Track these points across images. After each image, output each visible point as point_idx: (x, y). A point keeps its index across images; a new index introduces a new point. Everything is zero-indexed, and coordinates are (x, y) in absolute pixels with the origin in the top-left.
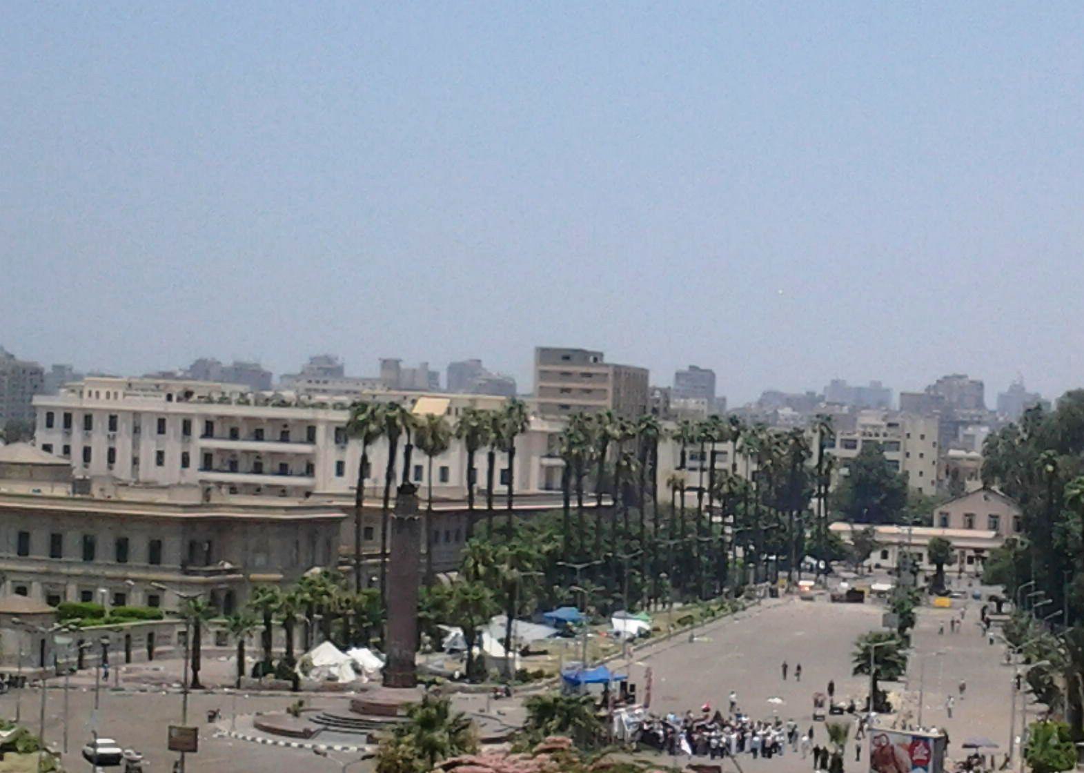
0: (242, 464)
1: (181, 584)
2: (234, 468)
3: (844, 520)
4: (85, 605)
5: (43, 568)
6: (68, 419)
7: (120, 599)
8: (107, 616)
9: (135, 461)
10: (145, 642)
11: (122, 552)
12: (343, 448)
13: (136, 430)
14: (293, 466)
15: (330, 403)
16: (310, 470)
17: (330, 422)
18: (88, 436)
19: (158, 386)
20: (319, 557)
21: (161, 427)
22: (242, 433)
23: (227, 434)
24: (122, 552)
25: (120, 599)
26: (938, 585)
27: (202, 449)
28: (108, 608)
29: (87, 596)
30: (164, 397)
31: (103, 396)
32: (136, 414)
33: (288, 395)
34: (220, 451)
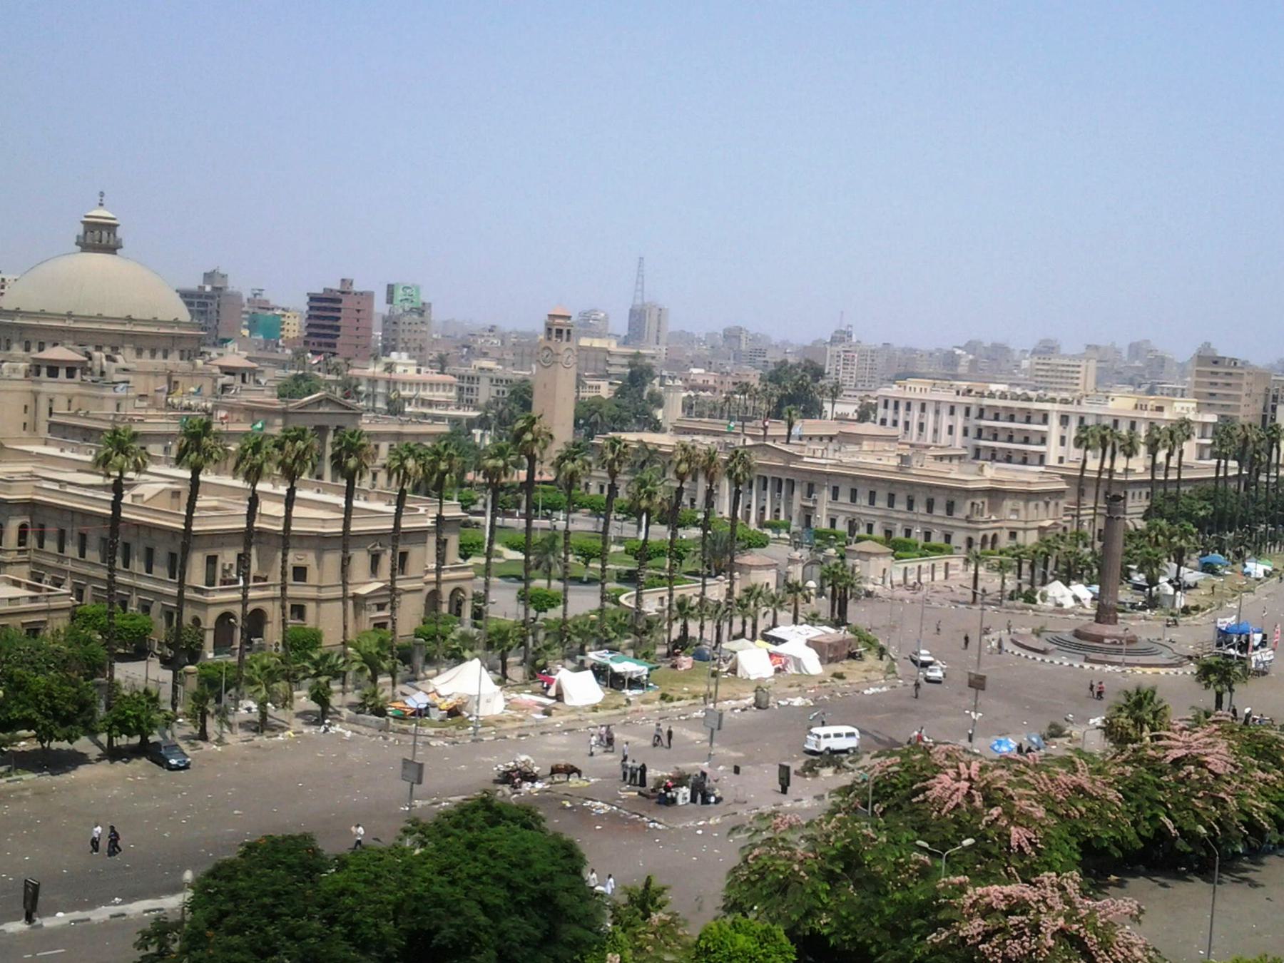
4: (907, 540)
7: (928, 536)
20: (1051, 516)
24: (930, 506)
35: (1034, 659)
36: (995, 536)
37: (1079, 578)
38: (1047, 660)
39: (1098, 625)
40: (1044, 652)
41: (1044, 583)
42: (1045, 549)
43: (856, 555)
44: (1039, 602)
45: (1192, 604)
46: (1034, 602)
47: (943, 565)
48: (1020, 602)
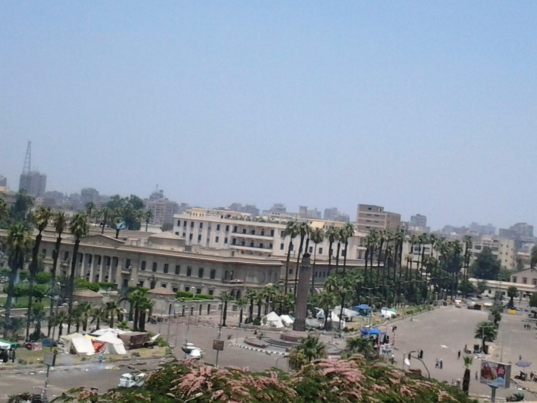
0: (247, 243)
1: (222, 287)
2: (243, 244)
3: (474, 277)
4: (186, 292)
5: (172, 278)
6: (185, 223)
7: (199, 291)
8: (194, 297)
9: (208, 240)
10: (207, 308)
11: (201, 273)
12: (284, 239)
13: (209, 228)
14: (265, 245)
15: (280, 222)
16: (271, 246)
17: (279, 229)
18: (192, 229)
19: (218, 212)
20: (272, 280)
21: (218, 228)
22: (247, 231)
23: (242, 231)
24: (201, 273)
25: (199, 291)
26: (511, 305)
27: (233, 236)
28: (194, 294)
29: (187, 289)
30: (220, 217)
31: (198, 215)
32: (210, 222)
33: (265, 218)
34: (239, 238)
35: (256, 350)
36: (239, 292)
37: (286, 313)
38: (264, 351)
39: (294, 331)
40: (263, 347)
41: (266, 314)
42: (267, 294)
43: (153, 296)
44: (262, 324)
45: (349, 328)
46: (260, 324)
47: (207, 306)
48: (251, 324)
